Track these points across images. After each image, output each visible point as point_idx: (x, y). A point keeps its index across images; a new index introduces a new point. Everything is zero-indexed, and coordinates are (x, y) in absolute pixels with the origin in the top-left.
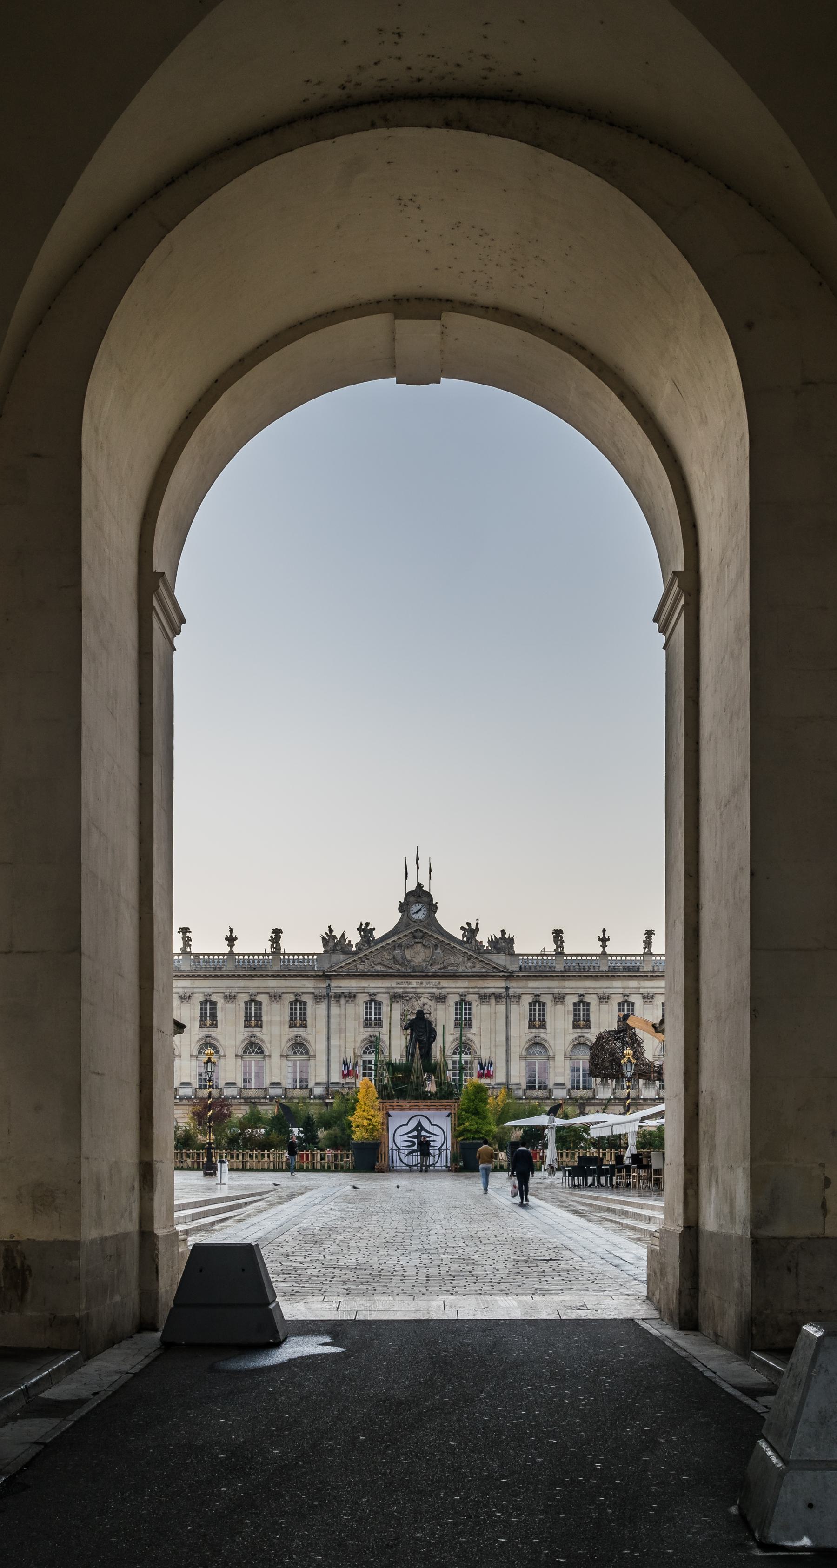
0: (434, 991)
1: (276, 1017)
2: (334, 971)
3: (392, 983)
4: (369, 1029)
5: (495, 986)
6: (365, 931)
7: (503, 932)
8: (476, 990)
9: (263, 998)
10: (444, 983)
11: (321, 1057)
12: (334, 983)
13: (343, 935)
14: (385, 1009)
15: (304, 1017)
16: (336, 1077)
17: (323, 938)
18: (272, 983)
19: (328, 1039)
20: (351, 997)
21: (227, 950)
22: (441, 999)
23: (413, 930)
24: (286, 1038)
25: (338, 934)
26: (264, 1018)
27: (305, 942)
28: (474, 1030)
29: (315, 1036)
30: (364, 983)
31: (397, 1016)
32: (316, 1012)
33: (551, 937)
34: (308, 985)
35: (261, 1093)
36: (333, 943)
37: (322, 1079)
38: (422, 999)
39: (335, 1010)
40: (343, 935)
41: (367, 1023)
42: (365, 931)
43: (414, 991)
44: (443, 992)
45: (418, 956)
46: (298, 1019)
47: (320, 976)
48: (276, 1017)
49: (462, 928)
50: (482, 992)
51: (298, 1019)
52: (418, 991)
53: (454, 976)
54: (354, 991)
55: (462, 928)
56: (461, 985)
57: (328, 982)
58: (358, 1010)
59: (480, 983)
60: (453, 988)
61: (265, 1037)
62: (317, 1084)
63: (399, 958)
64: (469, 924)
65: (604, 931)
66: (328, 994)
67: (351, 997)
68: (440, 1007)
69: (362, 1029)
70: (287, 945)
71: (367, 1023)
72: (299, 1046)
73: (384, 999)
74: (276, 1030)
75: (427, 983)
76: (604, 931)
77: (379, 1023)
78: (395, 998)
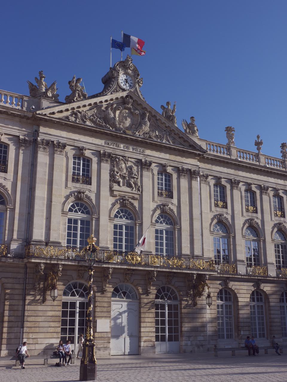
0: (140, 157)
2: (45, 115)
5: (191, 163)
8: (175, 164)
17: (31, 85)
43: (122, 153)
44: (148, 159)
47: (28, 118)
49: (162, 107)
50: (180, 166)
52: (127, 155)
54: (63, 141)
55: (162, 107)
57: (35, 128)
58: (64, 163)
59: (179, 159)
64: (168, 103)
65: (258, 137)
66: (35, 140)
69: (70, 184)
75: (133, 149)
76: (258, 137)
77: (88, 181)
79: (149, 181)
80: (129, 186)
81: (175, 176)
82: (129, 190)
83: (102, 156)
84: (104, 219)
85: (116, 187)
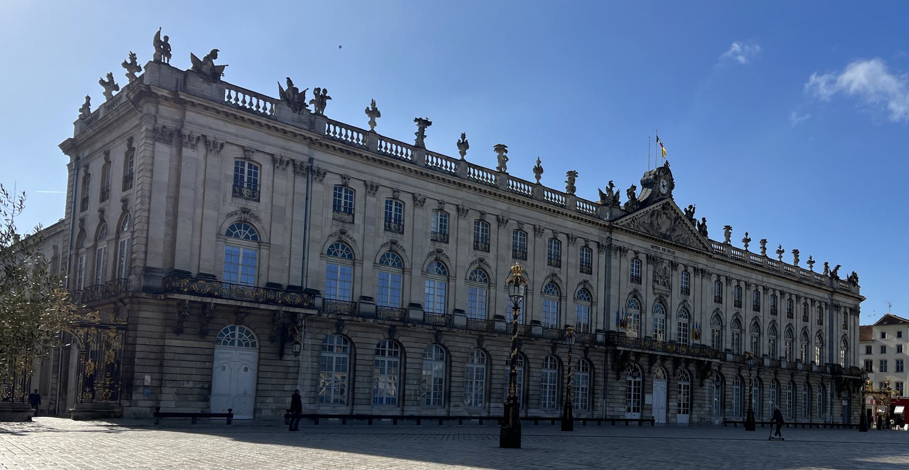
3: (647, 245)
4: (634, 284)
5: (702, 262)
6: (631, 192)
7: (704, 219)
9: (562, 238)
10: (678, 253)
11: (601, 305)
12: (614, 236)
13: (618, 193)
14: (644, 268)
16: (613, 327)
19: (607, 287)
23: (664, 201)
24: (578, 281)
25: (615, 190)
26: (564, 259)
28: (691, 297)
29: (597, 282)
31: (651, 277)
32: (599, 260)
33: (724, 232)
34: (594, 233)
36: (609, 199)
38: (664, 265)
39: (615, 262)
40: (618, 193)
45: (665, 224)
47: (605, 226)
48: (571, 256)
49: (685, 210)
53: (684, 248)
54: (626, 246)
55: (685, 210)
57: (608, 234)
60: (682, 257)
61: (563, 277)
62: (598, 331)
63: (655, 223)
64: (691, 207)
65: (747, 234)
66: (610, 245)
67: (622, 250)
68: (674, 272)
72: (585, 292)
73: (642, 257)
76: (747, 234)
78: (651, 259)
79: (677, 280)
80: (665, 285)
81: (692, 275)
82: (663, 288)
84: (649, 313)
85: (656, 286)
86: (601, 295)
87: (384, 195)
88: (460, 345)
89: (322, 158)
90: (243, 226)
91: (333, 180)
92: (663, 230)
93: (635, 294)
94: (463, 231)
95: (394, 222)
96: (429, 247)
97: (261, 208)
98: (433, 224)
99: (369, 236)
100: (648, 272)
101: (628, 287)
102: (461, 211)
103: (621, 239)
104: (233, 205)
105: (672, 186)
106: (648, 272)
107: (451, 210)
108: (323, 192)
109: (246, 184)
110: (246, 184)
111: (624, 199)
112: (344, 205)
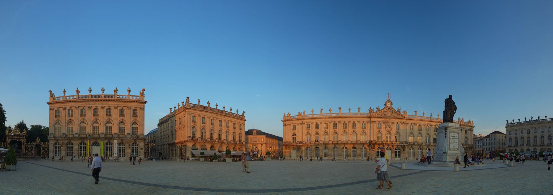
1: (359, 126)
3: (383, 119)
6: (378, 108)
9: (356, 122)
11: (369, 135)
15: (365, 126)
18: (358, 119)
20: (375, 122)
21: (414, 114)
22: (393, 123)
27: (365, 111)
29: (367, 130)
30: (378, 119)
32: (368, 125)
34: (366, 119)
35: (72, 136)
36: (371, 111)
37: (369, 139)
41: (378, 128)
42: (378, 108)
45: (389, 114)
46: (364, 127)
48: (359, 126)
51: (364, 127)
56: (397, 120)
58: (376, 125)
67: (375, 122)
70: (361, 111)
71: (378, 128)
74: (359, 128)
77: (381, 128)
78: (384, 122)
79: (394, 127)
83: (384, 122)
86: (368, 132)
87: (315, 124)
88: (416, 148)
89: (304, 121)
90: (294, 134)
91: (306, 124)
92: (389, 115)
93: (379, 131)
94: (331, 125)
95: (317, 127)
96: (323, 130)
97: (296, 131)
98: (325, 126)
99: (313, 131)
100: (383, 126)
101: (376, 130)
102: (330, 122)
103: (373, 119)
104: (292, 132)
105: (392, 104)
106: (383, 126)
107: (328, 123)
108: (305, 126)
109: (294, 129)
110: (294, 129)
111: (375, 110)
112: (308, 127)
